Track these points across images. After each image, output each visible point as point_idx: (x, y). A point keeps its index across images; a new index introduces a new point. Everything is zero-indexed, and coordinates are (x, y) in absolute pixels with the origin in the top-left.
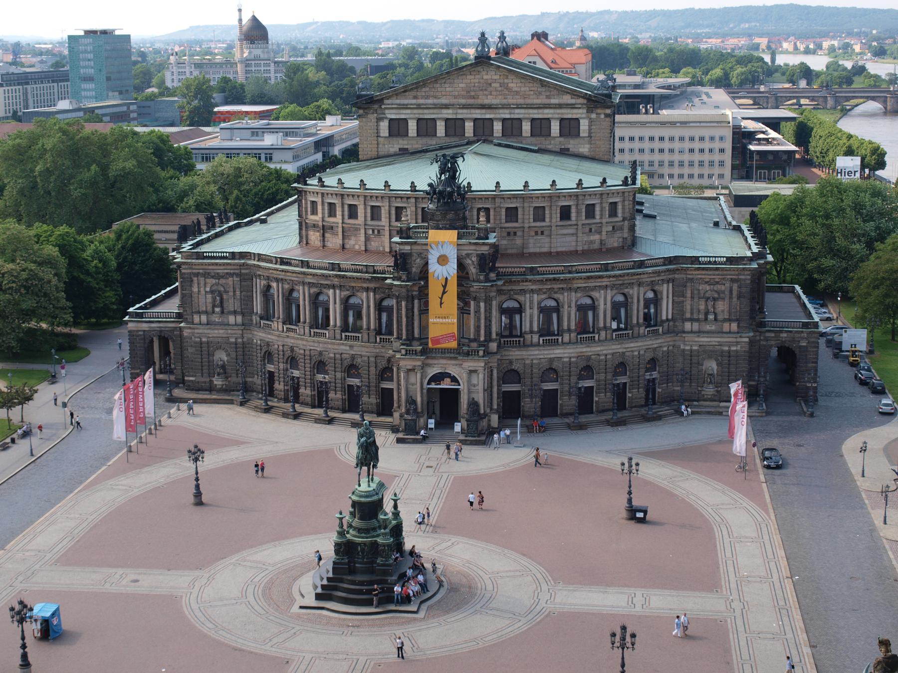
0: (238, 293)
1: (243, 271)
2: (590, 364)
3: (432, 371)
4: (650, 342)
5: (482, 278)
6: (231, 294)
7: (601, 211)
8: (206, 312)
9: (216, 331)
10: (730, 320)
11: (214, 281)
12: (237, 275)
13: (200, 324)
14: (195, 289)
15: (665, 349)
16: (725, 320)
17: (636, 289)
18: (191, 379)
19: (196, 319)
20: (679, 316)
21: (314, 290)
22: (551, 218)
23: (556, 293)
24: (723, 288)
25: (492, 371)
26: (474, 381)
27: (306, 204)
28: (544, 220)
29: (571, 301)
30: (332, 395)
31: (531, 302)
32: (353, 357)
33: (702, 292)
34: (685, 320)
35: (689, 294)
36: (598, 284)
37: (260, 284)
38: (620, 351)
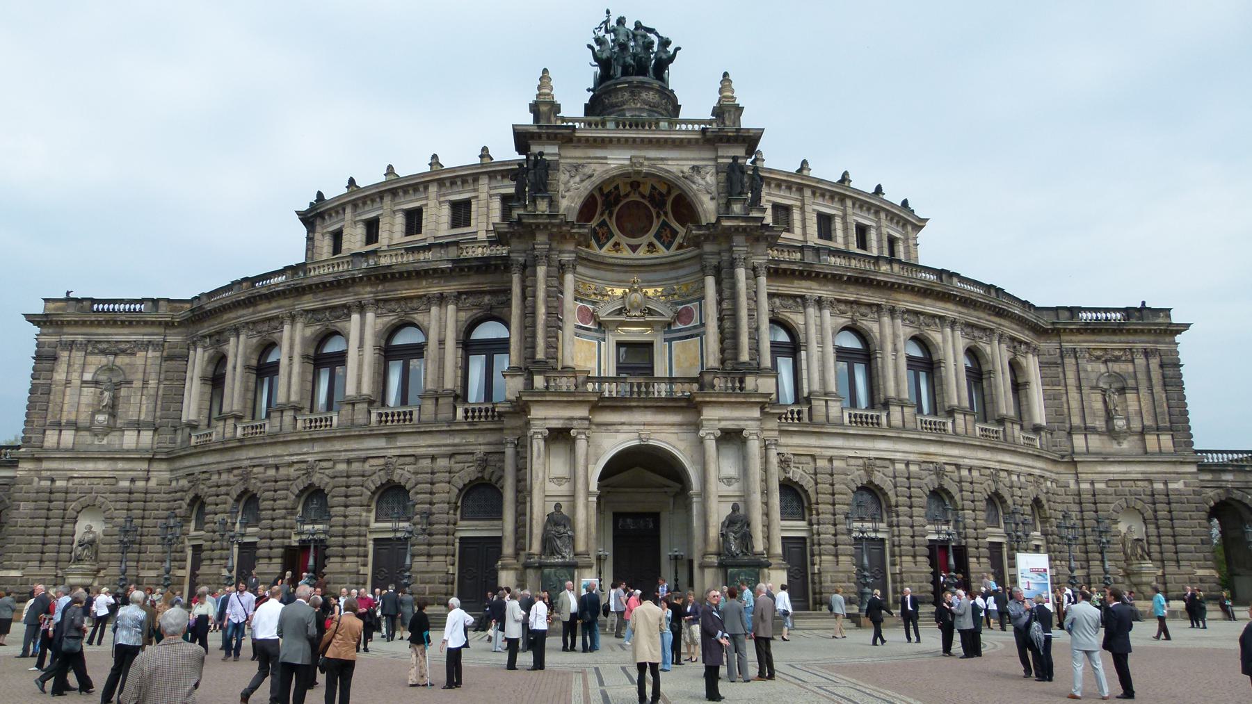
0: (153, 383)
1: (169, 339)
2: (948, 484)
4: (1029, 462)
6: (137, 384)
7: (880, 241)
9: (90, 465)
10: (1158, 430)
11: (103, 360)
14: (60, 376)
18: (13, 573)
19: (51, 438)
20: (1061, 425)
22: (804, 227)
23: (862, 315)
24: (1130, 367)
29: (895, 336)
33: (1093, 376)
35: (1071, 380)
37: (199, 359)
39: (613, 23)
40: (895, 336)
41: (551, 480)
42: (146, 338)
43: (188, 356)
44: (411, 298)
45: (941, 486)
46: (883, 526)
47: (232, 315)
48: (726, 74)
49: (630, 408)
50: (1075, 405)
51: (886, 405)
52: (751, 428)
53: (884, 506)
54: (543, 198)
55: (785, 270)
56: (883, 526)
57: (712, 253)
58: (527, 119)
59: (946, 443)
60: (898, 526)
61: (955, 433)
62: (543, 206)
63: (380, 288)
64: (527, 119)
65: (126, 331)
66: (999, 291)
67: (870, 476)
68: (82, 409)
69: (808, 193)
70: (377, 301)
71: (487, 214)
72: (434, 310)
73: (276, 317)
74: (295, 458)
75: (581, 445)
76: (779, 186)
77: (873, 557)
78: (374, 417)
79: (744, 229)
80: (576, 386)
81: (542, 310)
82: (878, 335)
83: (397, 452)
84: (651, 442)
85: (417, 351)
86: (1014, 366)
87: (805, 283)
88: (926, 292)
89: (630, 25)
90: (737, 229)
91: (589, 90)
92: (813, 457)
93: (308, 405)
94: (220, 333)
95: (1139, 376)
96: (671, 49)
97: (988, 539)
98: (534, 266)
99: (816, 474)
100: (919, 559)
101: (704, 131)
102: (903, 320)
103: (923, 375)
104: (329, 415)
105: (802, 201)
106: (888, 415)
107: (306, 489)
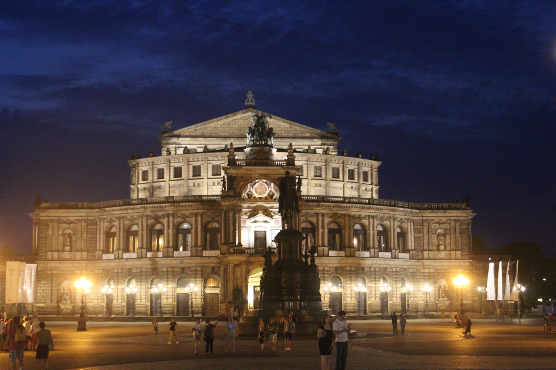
1: (90, 218)
8: (57, 251)
10: (456, 250)
11: (66, 226)
12: (85, 220)
13: (53, 260)
14: (50, 232)
15: (411, 270)
16: (451, 250)
18: (42, 305)
21: (151, 221)
33: (434, 230)
34: (423, 251)
36: (368, 214)
38: (385, 266)
42: (81, 218)
43: (97, 225)
47: (118, 212)
50: (426, 241)
65: (73, 215)
68: (59, 244)
70: (174, 214)
83: (183, 265)
87: (317, 208)
95: (452, 230)
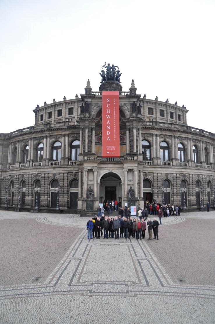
1: (4, 143)
2: (186, 178)
3: (103, 172)
4: (208, 172)
5: (134, 115)
7: (176, 116)
17: (201, 143)
22: (156, 114)
23: (167, 138)
25: (140, 173)
26: (131, 178)
27: (39, 117)
28: (152, 114)
29: (175, 143)
30: (42, 198)
31: (156, 142)
32: (54, 175)
37: (11, 148)
38: (198, 173)
39: (107, 65)
40: (175, 143)
41: (89, 181)
43: (8, 147)
44: (58, 135)
45: (185, 179)
46: (170, 189)
47: (18, 138)
48: (133, 80)
49: (107, 164)
51: (172, 160)
52: (135, 169)
53: (170, 184)
54: (87, 113)
55: (148, 128)
56: (170, 189)
57: (128, 125)
58: (84, 93)
59: (186, 169)
60: (173, 189)
61: (189, 166)
62: (87, 115)
63: (51, 132)
64: (84, 93)
66: (203, 131)
67: (167, 177)
69: (157, 105)
70: (50, 136)
71: (76, 114)
72: (63, 138)
73: (28, 139)
74: (33, 173)
75: (96, 173)
76: (150, 103)
77: (167, 197)
78: (50, 164)
79: (136, 120)
80: (94, 159)
81: (87, 140)
82: (171, 143)
83: (55, 172)
84: (112, 172)
85: (59, 147)
86: (206, 149)
88: (183, 132)
89: (111, 66)
90: (134, 120)
91: (100, 82)
92: (153, 173)
93: (35, 160)
94: (15, 142)
96: (120, 73)
97: (196, 191)
98: (85, 129)
99: (154, 177)
100: (178, 196)
101: (127, 95)
102: (177, 139)
103: (182, 152)
104: (40, 163)
105: (156, 107)
106: (172, 163)
107: (35, 180)
